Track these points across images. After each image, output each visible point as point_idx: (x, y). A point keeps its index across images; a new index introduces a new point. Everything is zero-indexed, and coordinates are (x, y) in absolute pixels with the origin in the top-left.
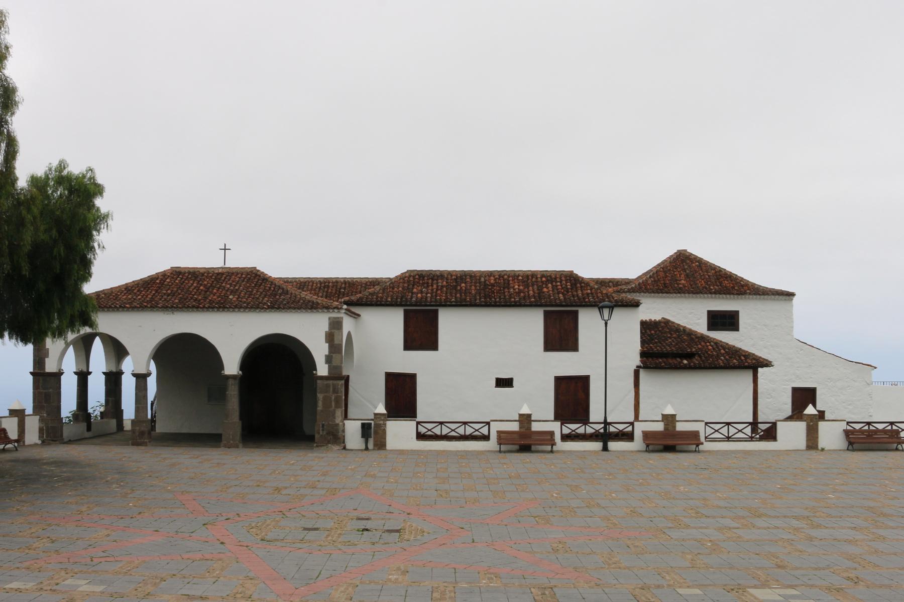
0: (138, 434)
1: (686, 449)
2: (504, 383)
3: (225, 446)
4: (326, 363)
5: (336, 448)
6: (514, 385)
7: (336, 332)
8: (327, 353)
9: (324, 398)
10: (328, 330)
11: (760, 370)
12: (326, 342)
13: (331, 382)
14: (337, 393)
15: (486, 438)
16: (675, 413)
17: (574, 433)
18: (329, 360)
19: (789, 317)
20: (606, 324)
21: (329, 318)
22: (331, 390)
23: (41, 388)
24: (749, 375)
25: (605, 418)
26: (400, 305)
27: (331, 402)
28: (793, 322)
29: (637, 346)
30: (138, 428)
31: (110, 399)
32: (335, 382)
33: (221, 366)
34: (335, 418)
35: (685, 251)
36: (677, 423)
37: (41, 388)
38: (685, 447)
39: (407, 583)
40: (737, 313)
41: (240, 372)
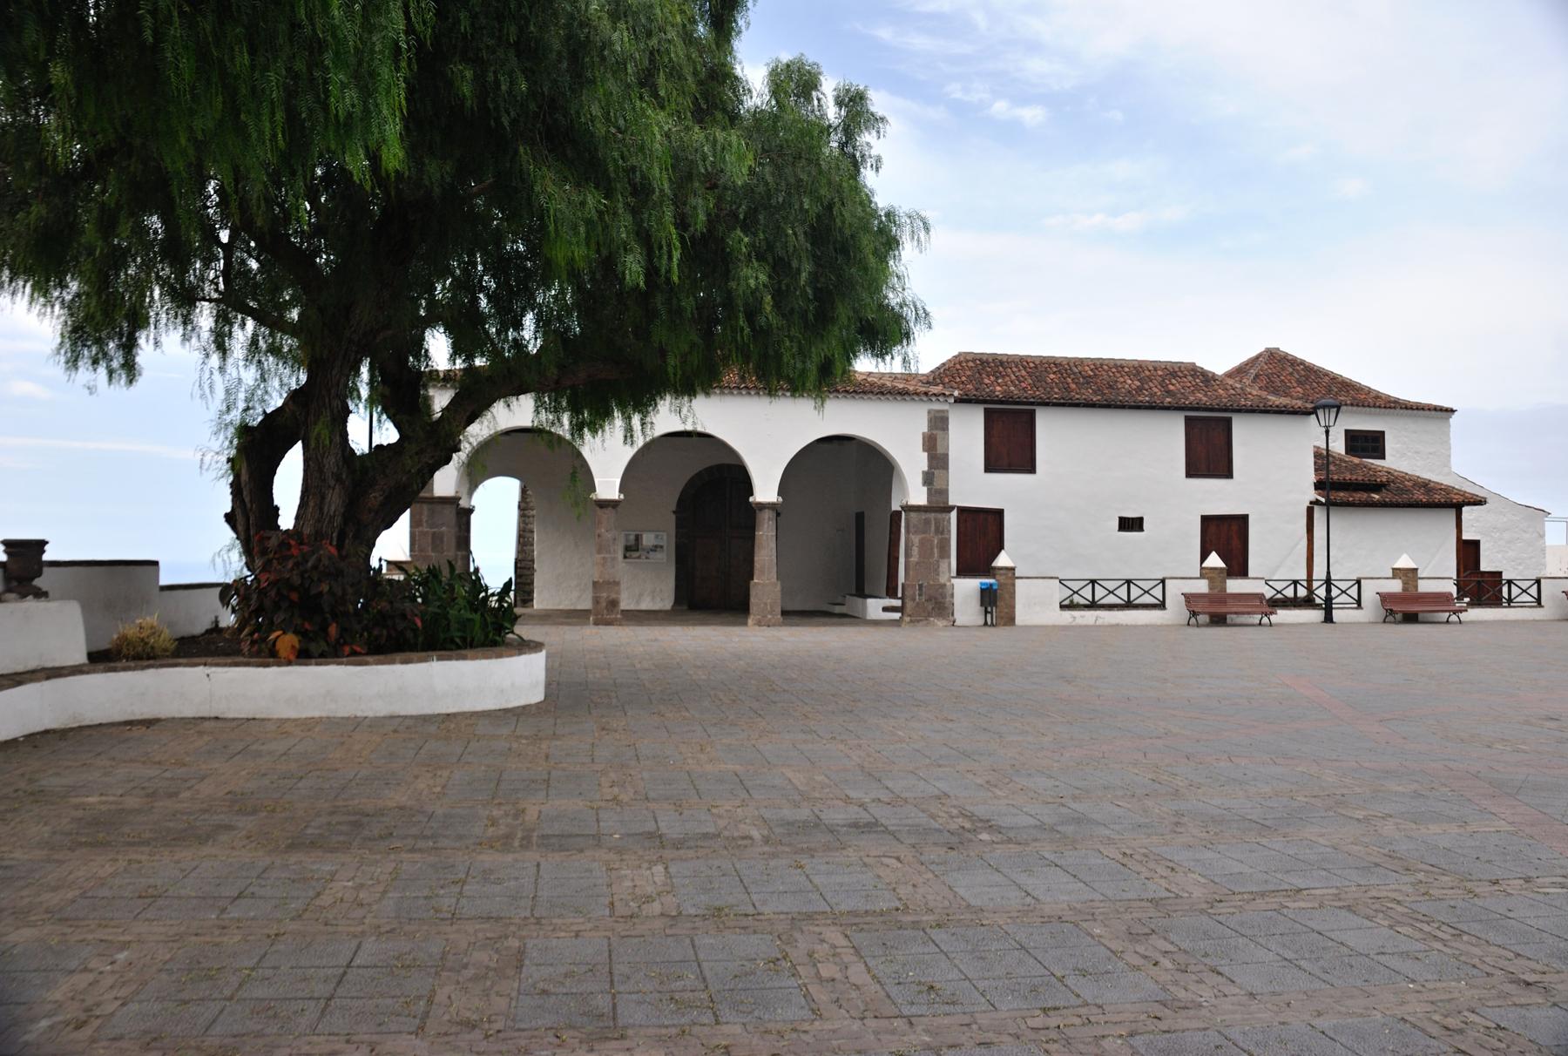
0: (604, 604)
1: (1430, 620)
2: (1130, 524)
3: (759, 624)
4: (924, 485)
5: (940, 623)
6: (1144, 528)
7: (939, 434)
8: (926, 469)
9: (922, 542)
10: (926, 430)
11: (1465, 509)
12: (924, 450)
13: (932, 516)
14: (942, 533)
15: (1162, 605)
16: (1413, 566)
17: (1279, 596)
18: (928, 479)
19: (1446, 443)
20: (1327, 432)
21: (929, 412)
22: (933, 528)
23: (425, 524)
24: (1452, 514)
25: (1328, 573)
26: (977, 401)
27: (932, 549)
28: (1450, 448)
29: (1311, 477)
30: (605, 595)
31: (459, 553)
32: (939, 516)
33: (749, 490)
34: (938, 575)
35: (1278, 349)
36: (1419, 581)
37: (425, 524)
38: (1430, 617)
39: (1264, 841)
40: (1383, 433)
41: (780, 499)
